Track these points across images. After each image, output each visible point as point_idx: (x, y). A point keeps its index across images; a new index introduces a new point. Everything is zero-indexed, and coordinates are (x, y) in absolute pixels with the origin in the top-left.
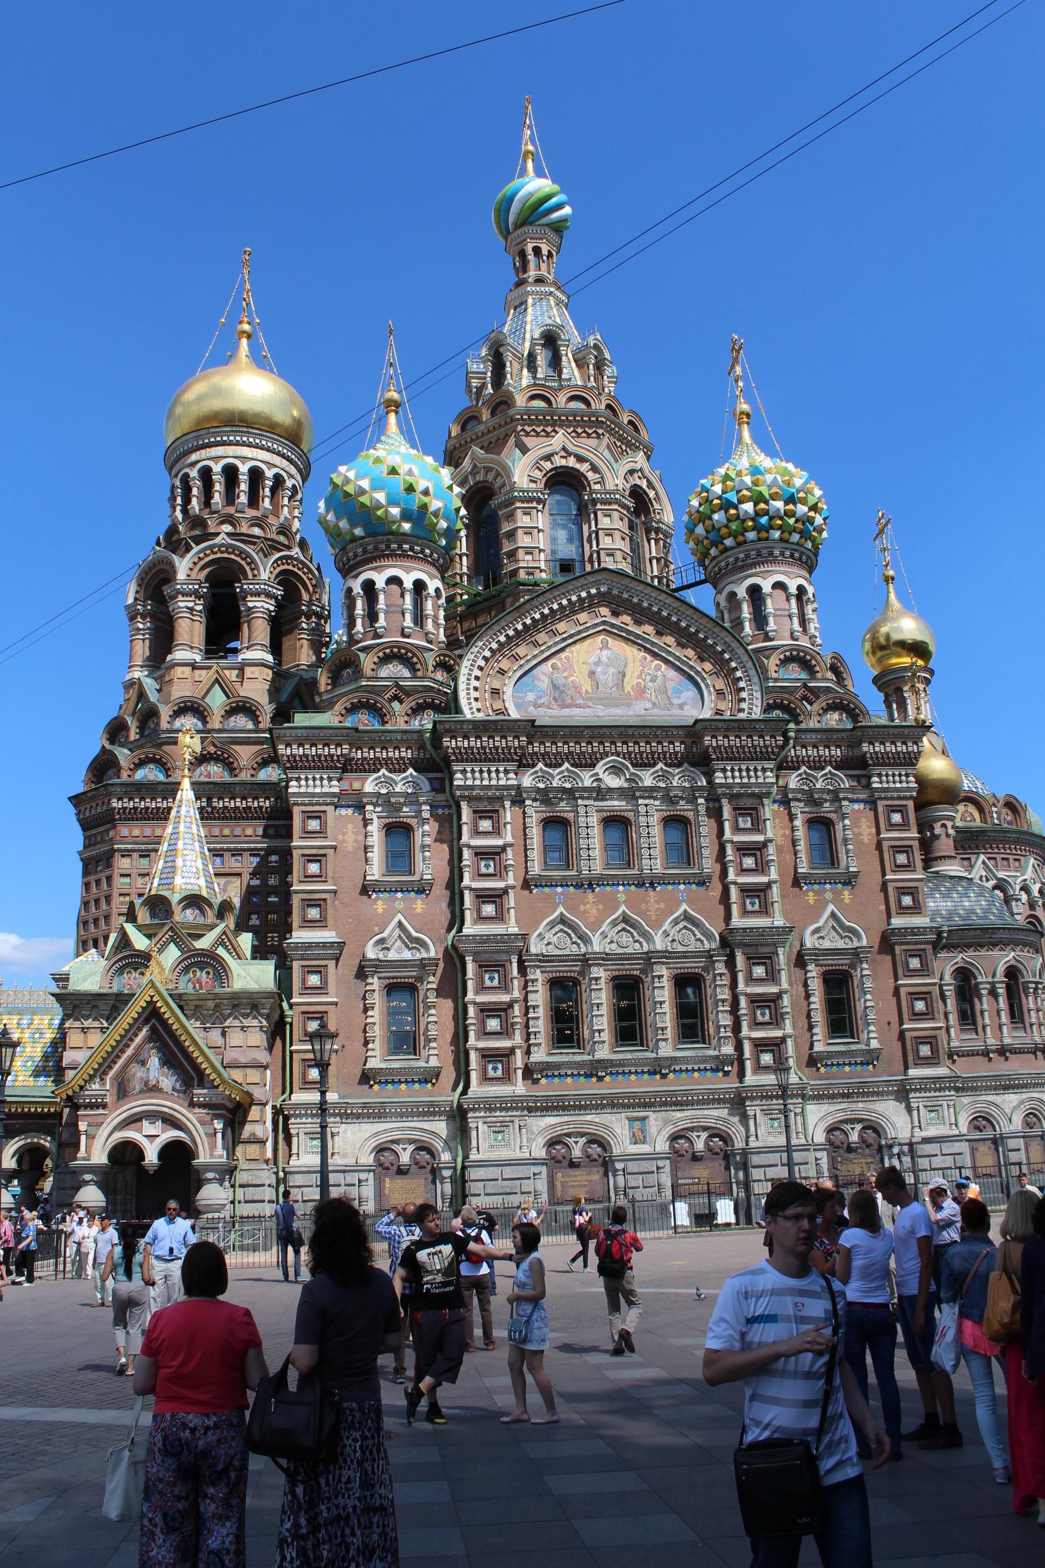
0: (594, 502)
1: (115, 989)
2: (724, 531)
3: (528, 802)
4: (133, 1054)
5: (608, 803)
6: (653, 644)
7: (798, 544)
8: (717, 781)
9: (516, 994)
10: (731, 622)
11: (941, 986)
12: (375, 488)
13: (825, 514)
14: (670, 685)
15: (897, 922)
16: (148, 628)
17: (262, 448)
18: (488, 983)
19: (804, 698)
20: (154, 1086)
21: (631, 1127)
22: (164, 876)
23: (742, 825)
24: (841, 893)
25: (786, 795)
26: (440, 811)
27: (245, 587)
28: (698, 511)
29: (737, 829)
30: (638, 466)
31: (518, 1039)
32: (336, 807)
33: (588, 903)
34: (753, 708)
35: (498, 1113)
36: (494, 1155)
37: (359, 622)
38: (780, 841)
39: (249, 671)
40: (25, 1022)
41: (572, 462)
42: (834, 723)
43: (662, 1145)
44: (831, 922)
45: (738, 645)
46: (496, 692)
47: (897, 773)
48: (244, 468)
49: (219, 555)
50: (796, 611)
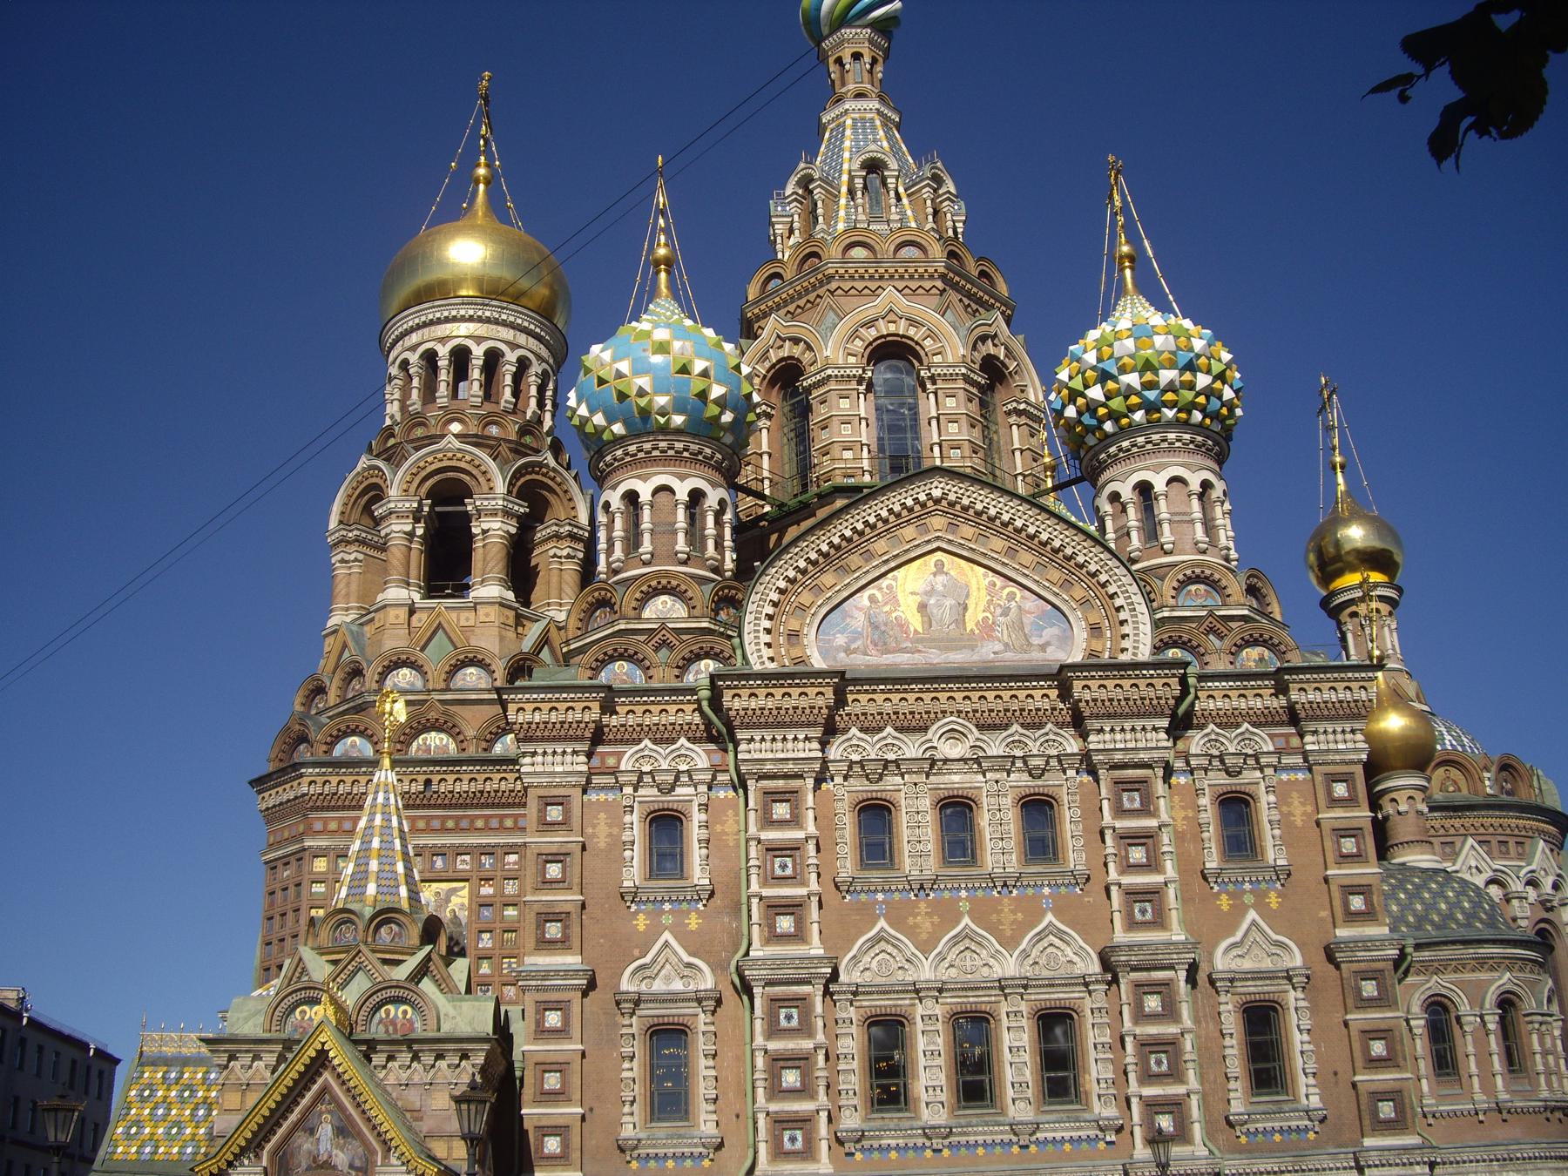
0: (933, 379)
1: (288, 1032)
2: (1102, 411)
3: (838, 780)
4: (299, 1120)
5: (946, 778)
6: (1004, 564)
7: (1201, 425)
8: (1091, 747)
9: (820, 1037)
10: (1115, 532)
11: (1407, 1021)
12: (637, 372)
13: (1237, 385)
14: (1028, 620)
15: (1342, 932)
16: (356, 560)
17: (504, 324)
18: (783, 1023)
19: (1211, 630)
22: (356, 883)
23: (1127, 805)
24: (1265, 894)
25: (1188, 763)
26: (722, 794)
27: (478, 503)
29: (1120, 811)
30: (992, 331)
31: (822, 1097)
32: (585, 792)
33: (919, 914)
34: (1140, 644)
37: (618, 546)
38: (1181, 826)
39: (482, 610)
40: (173, 1075)
41: (902, 328)
42: (1252, 664)
44: (1255, 934)
45: (1118, 564)
46: (794, 636)
47: (1339, 729)
48: (478, 351)
49: (446, 463)
50: (1200, 515)
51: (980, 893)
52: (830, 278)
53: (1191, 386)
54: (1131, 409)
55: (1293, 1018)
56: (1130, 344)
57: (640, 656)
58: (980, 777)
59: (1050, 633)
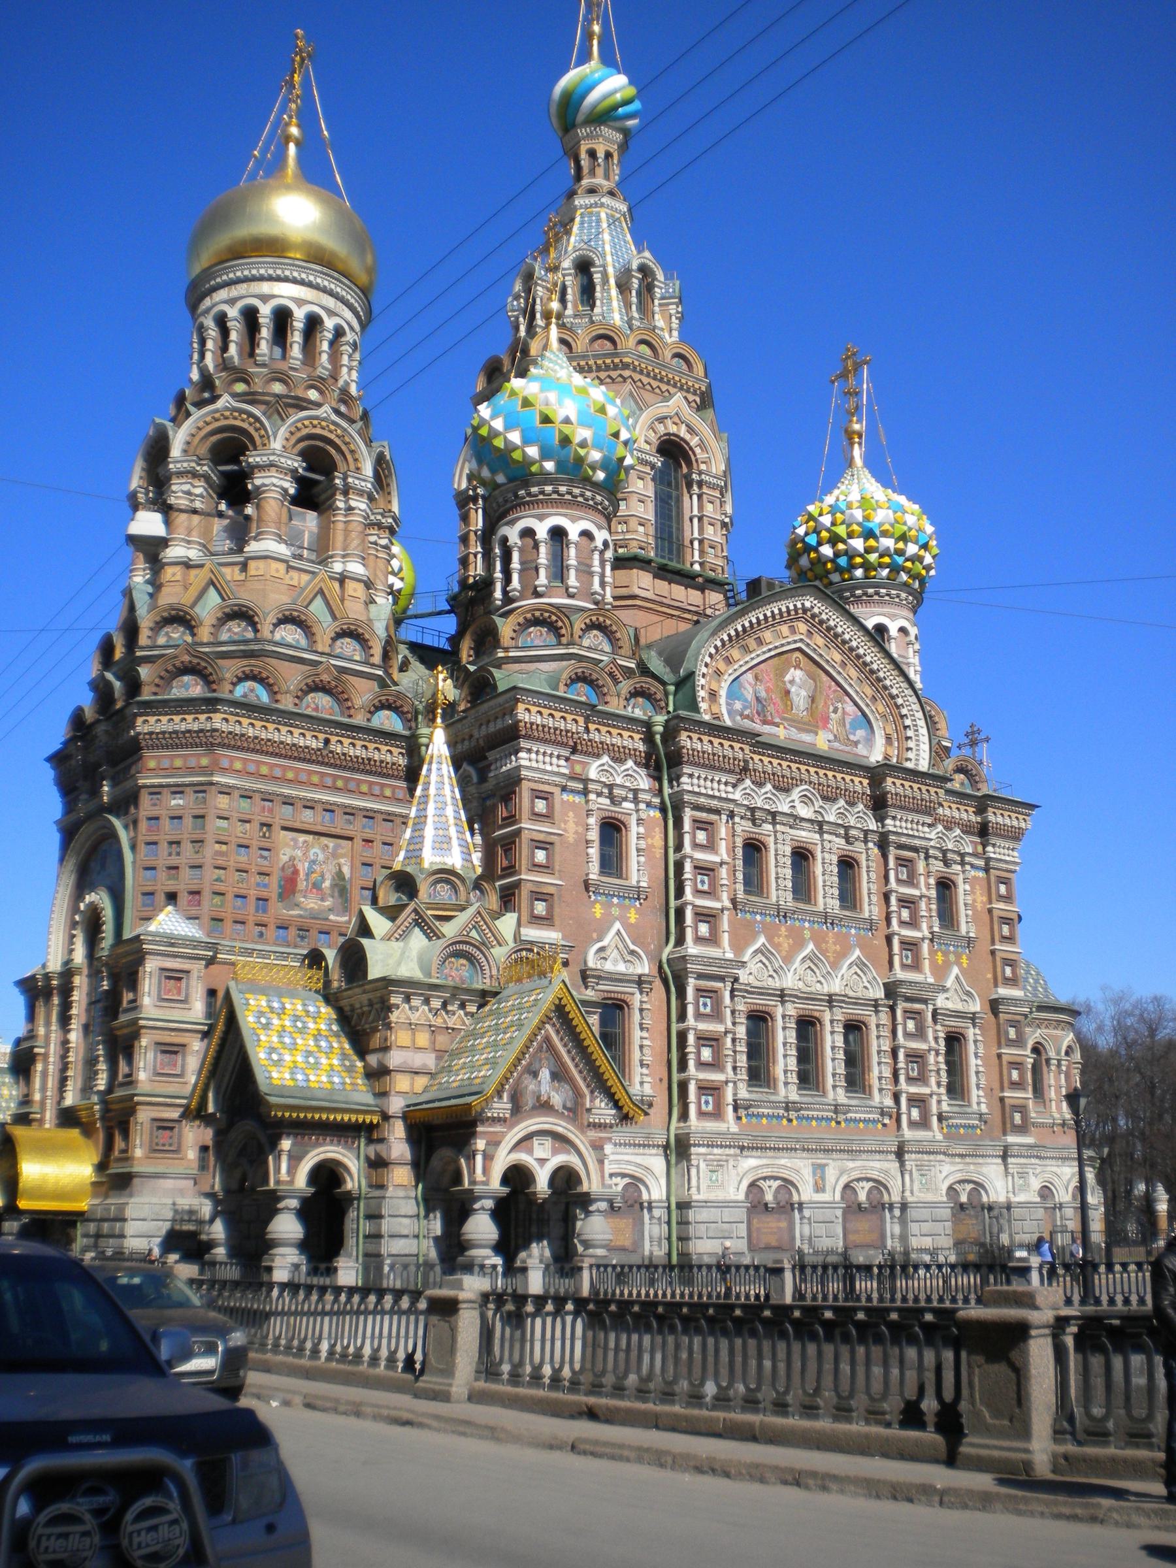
0: (700, 484)
12: (582, 424)
14: (848, 720)
15: (1003, 991)
16: (201, 496)
20: (546, 1102)
21: (814, 1174)
27: (350, 480)
28: (828, 530)
35: (716, 1151)
36: (712, 1196)
39: (351, 586)
41: (683, 432)
43: (838, 1197)
48: (329, 323)
49: (318, 431)
51: (816, 926)
52: (626, 366)
53: (920, 559)
54: (881, 566)
55: (971, 1048)
56: (890, 512)
57: (600, 683)
58: (817, 836)
59: (860, 734)
